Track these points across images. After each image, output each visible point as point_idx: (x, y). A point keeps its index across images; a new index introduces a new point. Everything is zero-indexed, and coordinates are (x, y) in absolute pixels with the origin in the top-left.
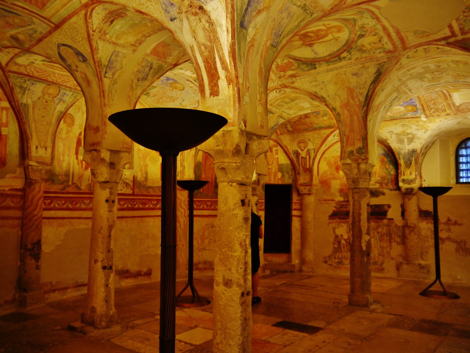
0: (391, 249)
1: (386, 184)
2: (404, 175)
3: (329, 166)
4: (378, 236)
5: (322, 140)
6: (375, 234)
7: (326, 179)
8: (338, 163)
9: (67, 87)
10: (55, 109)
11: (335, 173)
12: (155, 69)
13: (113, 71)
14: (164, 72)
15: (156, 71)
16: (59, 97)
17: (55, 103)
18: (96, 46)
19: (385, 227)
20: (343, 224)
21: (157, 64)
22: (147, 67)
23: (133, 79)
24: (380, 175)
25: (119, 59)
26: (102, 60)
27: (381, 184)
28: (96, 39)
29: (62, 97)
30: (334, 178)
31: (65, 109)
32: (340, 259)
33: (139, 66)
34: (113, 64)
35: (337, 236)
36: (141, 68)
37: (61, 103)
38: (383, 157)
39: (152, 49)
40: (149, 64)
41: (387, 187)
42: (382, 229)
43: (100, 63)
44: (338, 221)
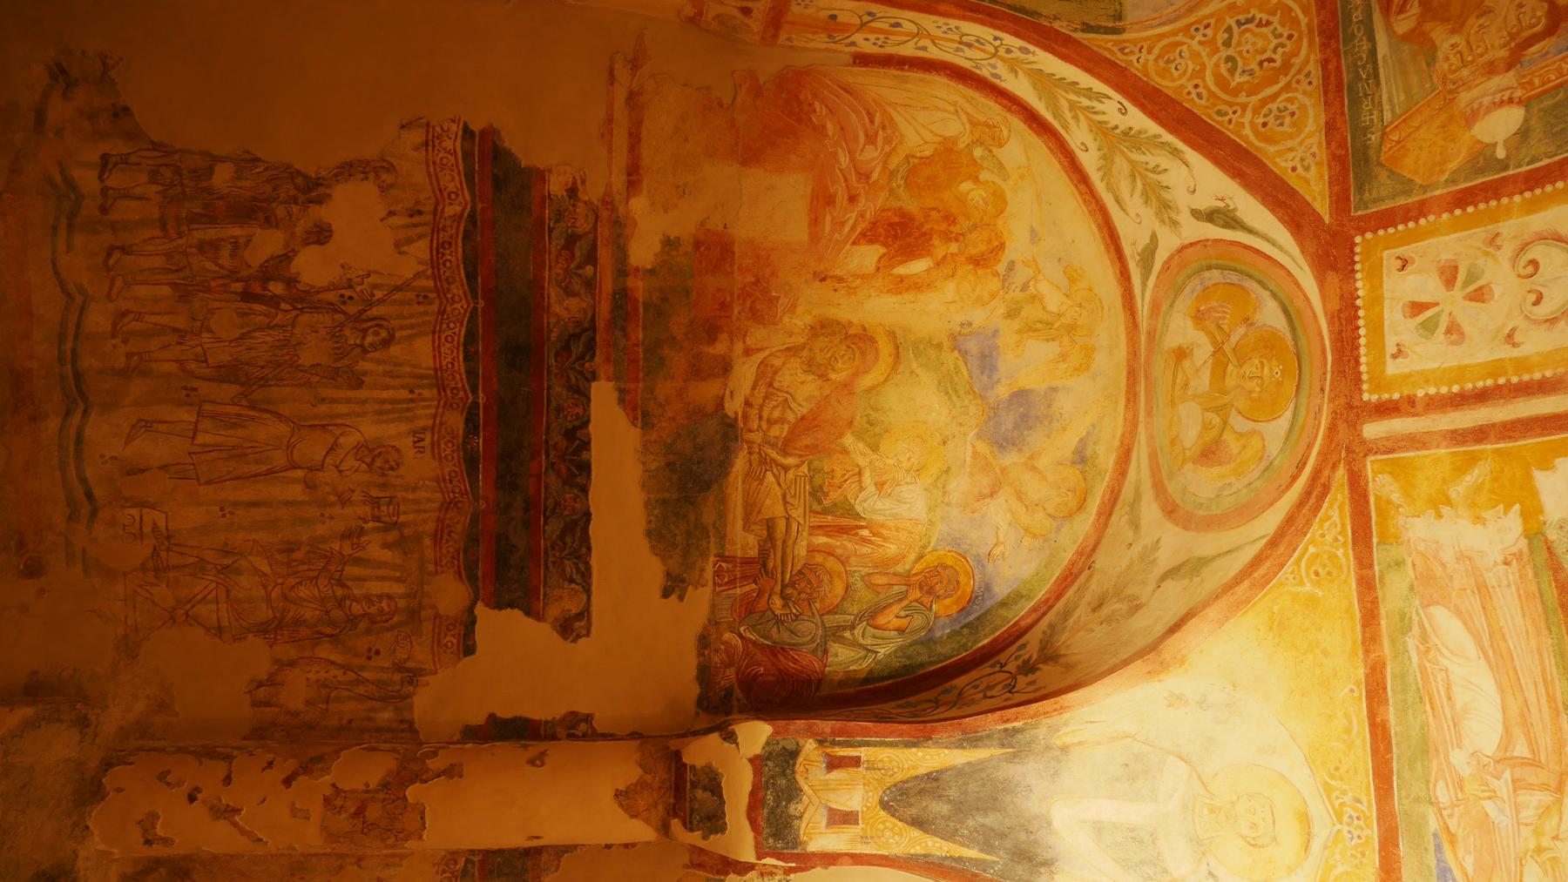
0: (219, 631)
1: (748, 608)
2: (834, 764)
3: (927, 161)
4: (320, 530)
5: (1199, 106)
6: (336, 510)
7: (821, 130)
8: (947, 237)
11: (870, 206)
19: (398, 589)
20: (421, 249)
24: (831, 563)
27: (758, 567)
30: (822, 200)
32: (104, 210)
35: (312, 190)
38: (968, 586)
41: (725, 615)
42: (379, 564)
44: (452, 210)
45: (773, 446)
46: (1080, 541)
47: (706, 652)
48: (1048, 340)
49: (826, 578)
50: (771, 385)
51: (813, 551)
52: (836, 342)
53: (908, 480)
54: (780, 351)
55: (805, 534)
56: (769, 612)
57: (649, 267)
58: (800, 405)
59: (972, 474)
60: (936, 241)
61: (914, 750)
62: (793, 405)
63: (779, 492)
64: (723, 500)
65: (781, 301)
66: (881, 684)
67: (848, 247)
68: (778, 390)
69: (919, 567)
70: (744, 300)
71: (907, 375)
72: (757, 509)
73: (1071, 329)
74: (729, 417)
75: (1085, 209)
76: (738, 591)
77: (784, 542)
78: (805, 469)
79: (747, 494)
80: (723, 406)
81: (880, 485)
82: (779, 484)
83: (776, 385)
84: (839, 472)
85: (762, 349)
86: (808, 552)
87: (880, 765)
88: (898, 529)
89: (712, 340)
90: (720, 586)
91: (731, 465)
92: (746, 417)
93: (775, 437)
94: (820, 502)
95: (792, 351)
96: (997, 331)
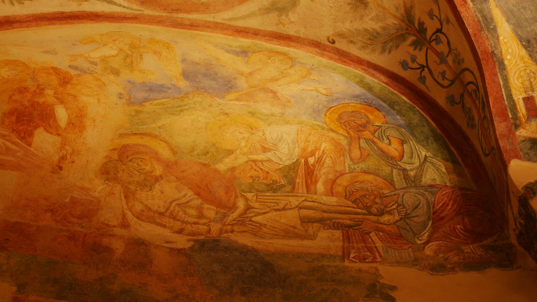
45: (225, 216)
46: (312, 55)
47: (449, 266)
48: (141, 58)
49: (358, 186)
50: (161, 214)
51: (332, 193)
52: (124, 167)
53: (261, 134)
54: (127, 203)
55: (315, 197)
56: (398, 224)
57: (15, 289)
58: (185, 196)
59: (256, 102)
60: (41, 100)
61: (506, 62)
62: (184, 200)
63: (272, 215)
64: (283, 254)
65: (74, 195)
66: (457, 155)
67: (32, 149)
68: (167, 210)
69: (341, 131)
70: (70, 223)
71: (162, 130)
72: (292, 229)
73: (132, 46)
74: (193, 246)
75: (33, 28)
76: (379, 244)
77: (324, 211)
78: (249, 195)
79: (276, 236)
80: (181, 249)
81: (265, 150)
82: (265, 213)
83: (162, 210)
84: (253, 173)
85: (124, 215)
86: (333, 196)
87: (527, 83)
88: (307, 141)
89: (109, 250)
90: (375, 258)
91: (245, 246)
92: (194, 234)
93: (216, 213)
94: (283, 186)
95: (128, 195)
96: (129, 82)
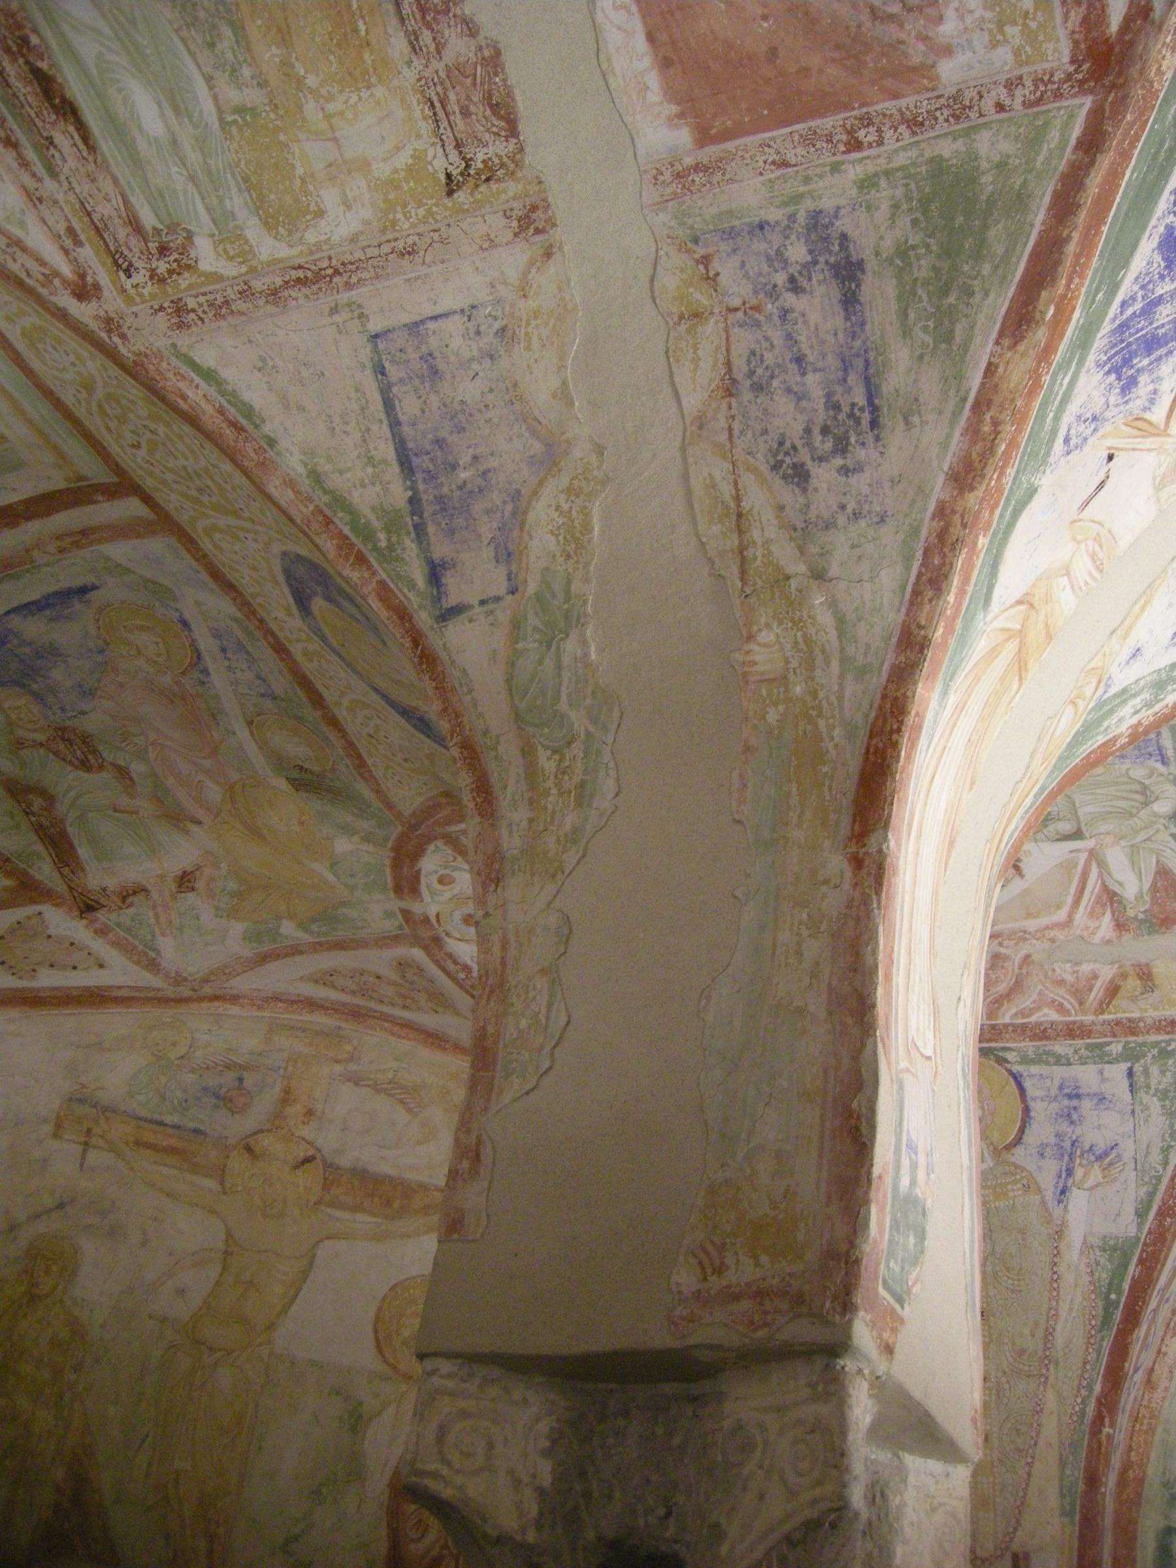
9: (1042, 1033)
10: (1059, 1233)
12: (903, 252)
13: (487, 528)
14: (1039, 218)
15: (922, 269)
16: (1041, 1131)
17: (1039, 1190)
18: (212, 391)
21: (884, 194)
22: (795, 286)
23: (726, 490)
25: (469, 391)
26: (335, 481)
28: (161, 343)
29: (1065, 1127)
31: (1141, 1214)
33: (711, 329)
34: (454, 467)
36: (744, 340)
37: (1089, 1175)
39: (653, 80)
40: (798, 252)
43: (341, 521)
